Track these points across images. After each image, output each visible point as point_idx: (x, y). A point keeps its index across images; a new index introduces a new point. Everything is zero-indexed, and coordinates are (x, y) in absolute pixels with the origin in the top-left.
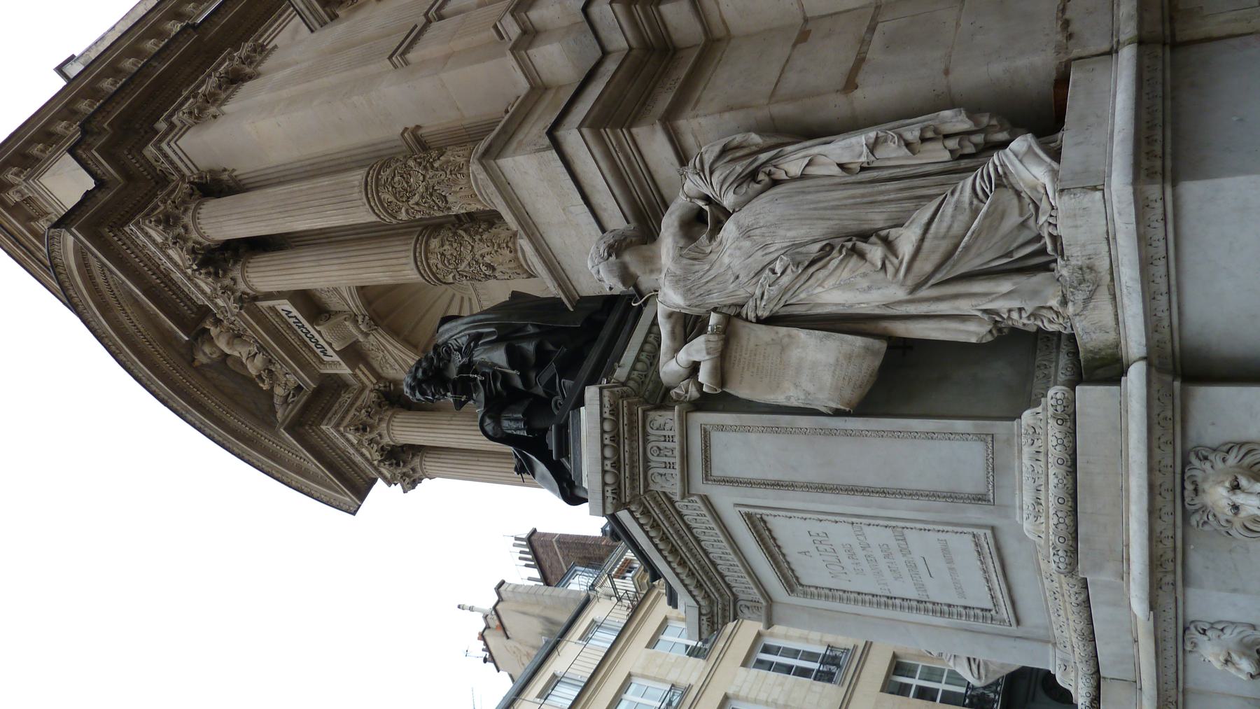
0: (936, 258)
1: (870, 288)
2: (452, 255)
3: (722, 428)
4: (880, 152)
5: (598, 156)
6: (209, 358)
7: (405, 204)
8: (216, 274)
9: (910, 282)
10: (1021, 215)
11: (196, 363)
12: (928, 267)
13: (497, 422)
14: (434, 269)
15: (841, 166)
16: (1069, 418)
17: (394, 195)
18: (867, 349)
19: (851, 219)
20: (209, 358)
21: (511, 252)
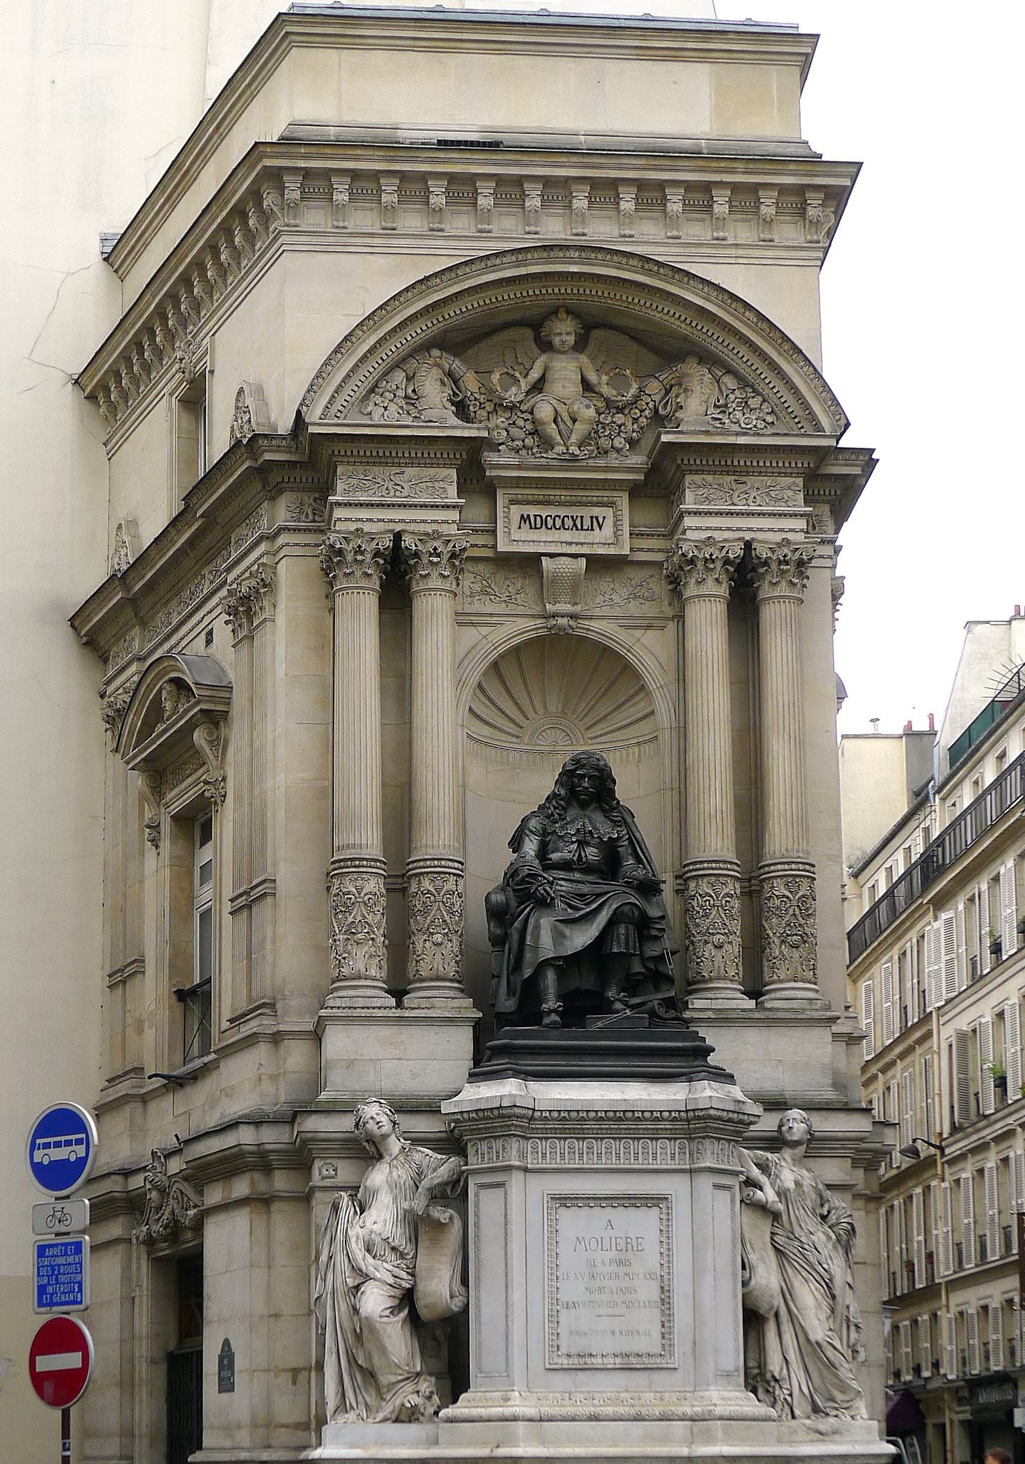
0: (832, 1358)
1: (819, 1320)
2: (733, 908)
3: (733, 1201)
4: (853, 1328)
5: (847, 1134)
6: (560, 334)
7: (794, 903)
8: (727, 561)
9: (825, 1344)
10: (842, 1401)
11: (563, 315)
12: (828, 1354)
13: (629, 920)
14: (722, 879)
15: (848, 1307)
16: (767, 1419)
17: (803, 896)
18: (772, 1307)
19: (840, 1310)
20: (560, 334)
21: (733, 976)
